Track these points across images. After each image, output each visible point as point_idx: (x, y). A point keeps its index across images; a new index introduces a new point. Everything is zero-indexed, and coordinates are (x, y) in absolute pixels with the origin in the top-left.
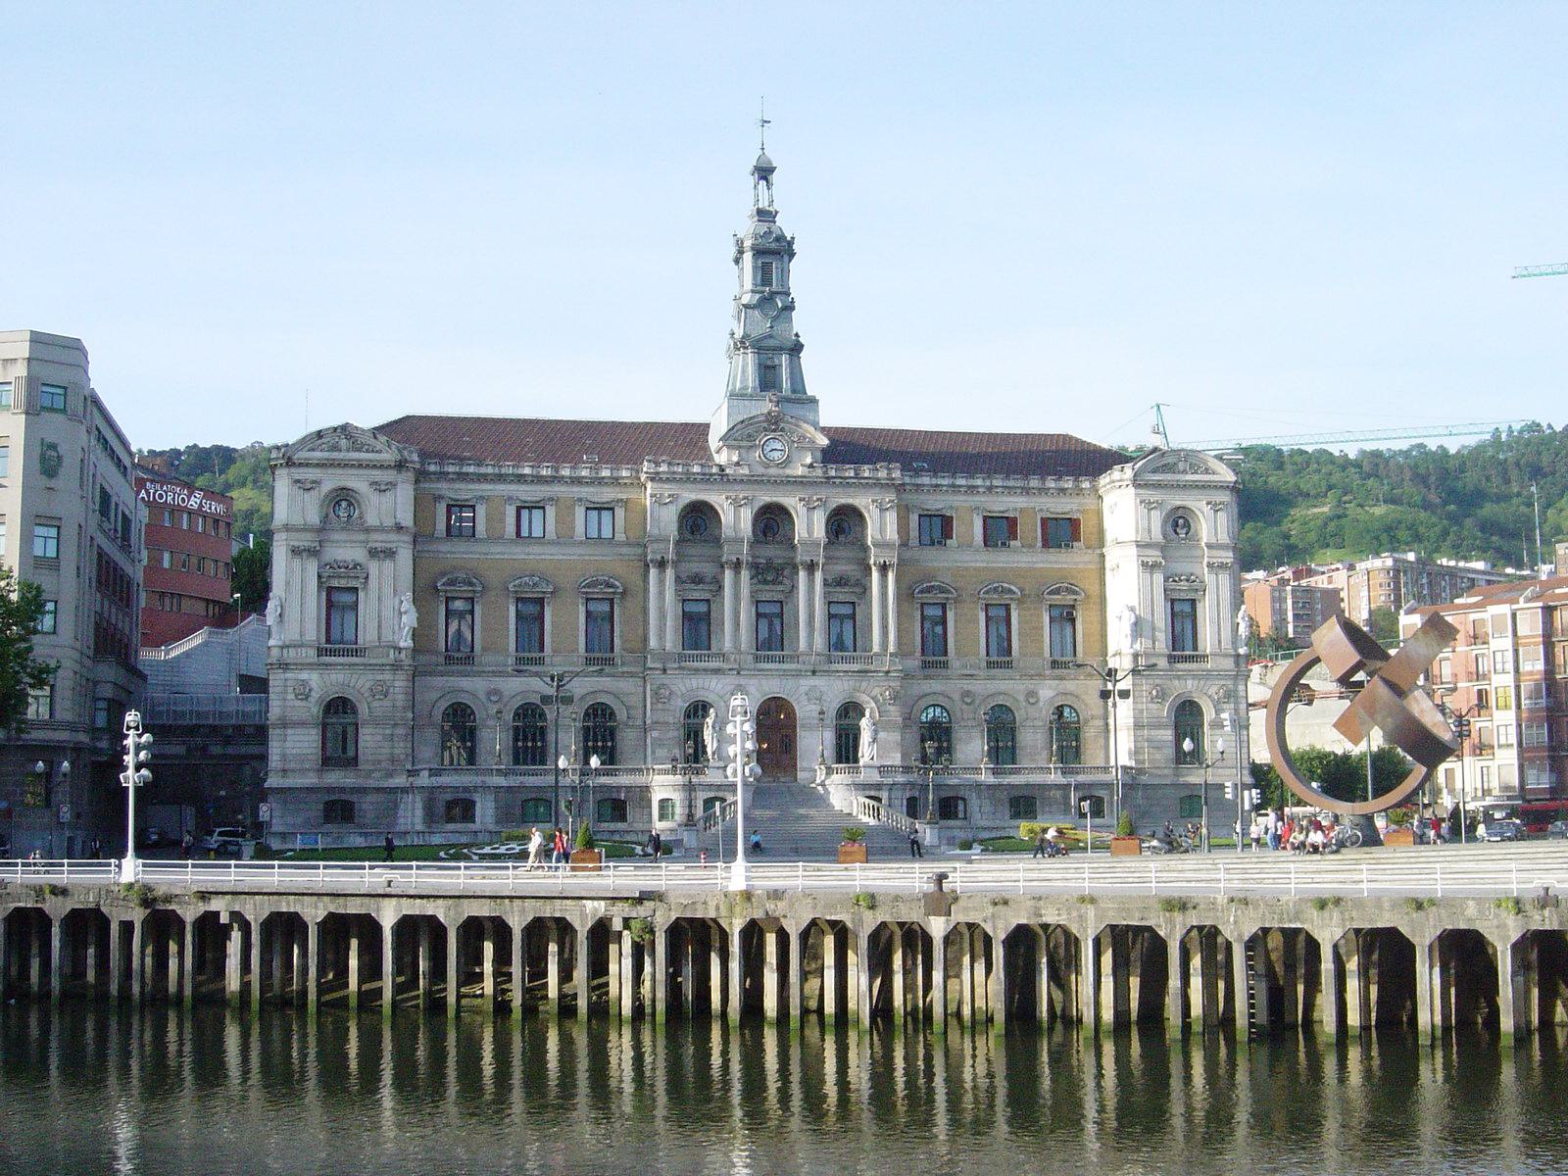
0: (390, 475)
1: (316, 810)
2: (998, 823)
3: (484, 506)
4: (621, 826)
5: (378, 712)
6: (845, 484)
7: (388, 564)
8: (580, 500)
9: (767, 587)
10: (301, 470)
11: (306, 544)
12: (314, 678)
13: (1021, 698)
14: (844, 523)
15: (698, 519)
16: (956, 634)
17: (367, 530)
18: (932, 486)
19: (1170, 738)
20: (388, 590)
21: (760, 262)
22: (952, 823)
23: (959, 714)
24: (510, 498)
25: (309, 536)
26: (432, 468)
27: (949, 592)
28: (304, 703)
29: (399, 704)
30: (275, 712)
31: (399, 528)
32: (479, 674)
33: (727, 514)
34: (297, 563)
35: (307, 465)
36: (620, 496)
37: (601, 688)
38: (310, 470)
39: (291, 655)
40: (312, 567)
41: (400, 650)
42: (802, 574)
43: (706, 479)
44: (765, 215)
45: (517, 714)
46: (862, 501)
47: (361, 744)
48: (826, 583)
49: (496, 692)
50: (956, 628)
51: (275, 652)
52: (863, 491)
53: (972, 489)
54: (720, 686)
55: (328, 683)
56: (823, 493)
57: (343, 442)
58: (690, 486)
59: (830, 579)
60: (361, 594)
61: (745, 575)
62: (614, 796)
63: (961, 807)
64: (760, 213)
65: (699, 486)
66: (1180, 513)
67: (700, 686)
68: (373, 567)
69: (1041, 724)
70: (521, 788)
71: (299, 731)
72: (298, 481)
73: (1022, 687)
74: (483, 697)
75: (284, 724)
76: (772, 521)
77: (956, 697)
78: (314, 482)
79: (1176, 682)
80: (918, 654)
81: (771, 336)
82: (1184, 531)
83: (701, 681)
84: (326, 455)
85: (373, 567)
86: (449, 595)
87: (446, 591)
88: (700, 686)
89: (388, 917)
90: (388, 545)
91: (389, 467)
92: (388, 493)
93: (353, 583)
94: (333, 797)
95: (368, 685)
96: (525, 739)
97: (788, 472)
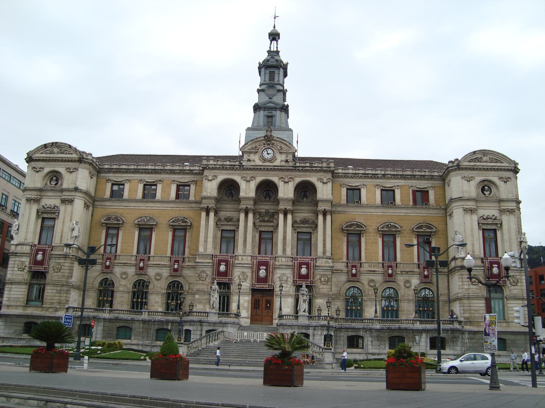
0: (76, 165)
1: (20, 327)
3: (129, 184)
5: (55, 278)
6: (304, 170)
7: (69, 207)
8: (174, 181)
11: (33, 196)
14: (305, 191)
16: (366, 249)
17: (62, 191)
18: (353, 174)
19: (484, 305)
20: (68, 219)
21: (268, 71)
22: (355, 350)
23: (367, 292)
24: (141, 180)
25: (35, 193)
26: (106, 167)
27: (362, 227)
28: (22, 273)
29: (66, 275)
30: (9, 276)
31: (76, 189)
34: (28, 206)
35: (39, 160)
36: (193, 179)
39: (19, 248)
40: (35, 207)
42: (281, 216)
43: (232, 168)
44: (273, 54)
45: (135, 285)
46: (313, 179)
47: (46, 294)
48: (294, 222)
49: (125, 273)
50: (366, 246)
52: (314, 174)
53: (375, 176)
56: (293, 174)
57: (56, 150)
59: (298, 220)
60: (56, 221)
61: (251, 216)
62: (165, 327)
63: (360, 341)
64: (269, 52)
65: (229, 172)
66: (486, 183)
68: (62, 208)
69: (412, 298)
70: (117, 319)
71: (17, 286)
72: (34, 168)
75: (12, 283)
76: (267, 189)
78: (41, 168)
80: (345, 260)
81: (271, 102)
82: (488, 193)
84: (48, 155)
85: (62, 208)
86: (108, 226)
87: (106, 224)
90: (70, 197)
91: (75, 161)
92: (73, 173)
93: (53, 216)
94: (31, 320)
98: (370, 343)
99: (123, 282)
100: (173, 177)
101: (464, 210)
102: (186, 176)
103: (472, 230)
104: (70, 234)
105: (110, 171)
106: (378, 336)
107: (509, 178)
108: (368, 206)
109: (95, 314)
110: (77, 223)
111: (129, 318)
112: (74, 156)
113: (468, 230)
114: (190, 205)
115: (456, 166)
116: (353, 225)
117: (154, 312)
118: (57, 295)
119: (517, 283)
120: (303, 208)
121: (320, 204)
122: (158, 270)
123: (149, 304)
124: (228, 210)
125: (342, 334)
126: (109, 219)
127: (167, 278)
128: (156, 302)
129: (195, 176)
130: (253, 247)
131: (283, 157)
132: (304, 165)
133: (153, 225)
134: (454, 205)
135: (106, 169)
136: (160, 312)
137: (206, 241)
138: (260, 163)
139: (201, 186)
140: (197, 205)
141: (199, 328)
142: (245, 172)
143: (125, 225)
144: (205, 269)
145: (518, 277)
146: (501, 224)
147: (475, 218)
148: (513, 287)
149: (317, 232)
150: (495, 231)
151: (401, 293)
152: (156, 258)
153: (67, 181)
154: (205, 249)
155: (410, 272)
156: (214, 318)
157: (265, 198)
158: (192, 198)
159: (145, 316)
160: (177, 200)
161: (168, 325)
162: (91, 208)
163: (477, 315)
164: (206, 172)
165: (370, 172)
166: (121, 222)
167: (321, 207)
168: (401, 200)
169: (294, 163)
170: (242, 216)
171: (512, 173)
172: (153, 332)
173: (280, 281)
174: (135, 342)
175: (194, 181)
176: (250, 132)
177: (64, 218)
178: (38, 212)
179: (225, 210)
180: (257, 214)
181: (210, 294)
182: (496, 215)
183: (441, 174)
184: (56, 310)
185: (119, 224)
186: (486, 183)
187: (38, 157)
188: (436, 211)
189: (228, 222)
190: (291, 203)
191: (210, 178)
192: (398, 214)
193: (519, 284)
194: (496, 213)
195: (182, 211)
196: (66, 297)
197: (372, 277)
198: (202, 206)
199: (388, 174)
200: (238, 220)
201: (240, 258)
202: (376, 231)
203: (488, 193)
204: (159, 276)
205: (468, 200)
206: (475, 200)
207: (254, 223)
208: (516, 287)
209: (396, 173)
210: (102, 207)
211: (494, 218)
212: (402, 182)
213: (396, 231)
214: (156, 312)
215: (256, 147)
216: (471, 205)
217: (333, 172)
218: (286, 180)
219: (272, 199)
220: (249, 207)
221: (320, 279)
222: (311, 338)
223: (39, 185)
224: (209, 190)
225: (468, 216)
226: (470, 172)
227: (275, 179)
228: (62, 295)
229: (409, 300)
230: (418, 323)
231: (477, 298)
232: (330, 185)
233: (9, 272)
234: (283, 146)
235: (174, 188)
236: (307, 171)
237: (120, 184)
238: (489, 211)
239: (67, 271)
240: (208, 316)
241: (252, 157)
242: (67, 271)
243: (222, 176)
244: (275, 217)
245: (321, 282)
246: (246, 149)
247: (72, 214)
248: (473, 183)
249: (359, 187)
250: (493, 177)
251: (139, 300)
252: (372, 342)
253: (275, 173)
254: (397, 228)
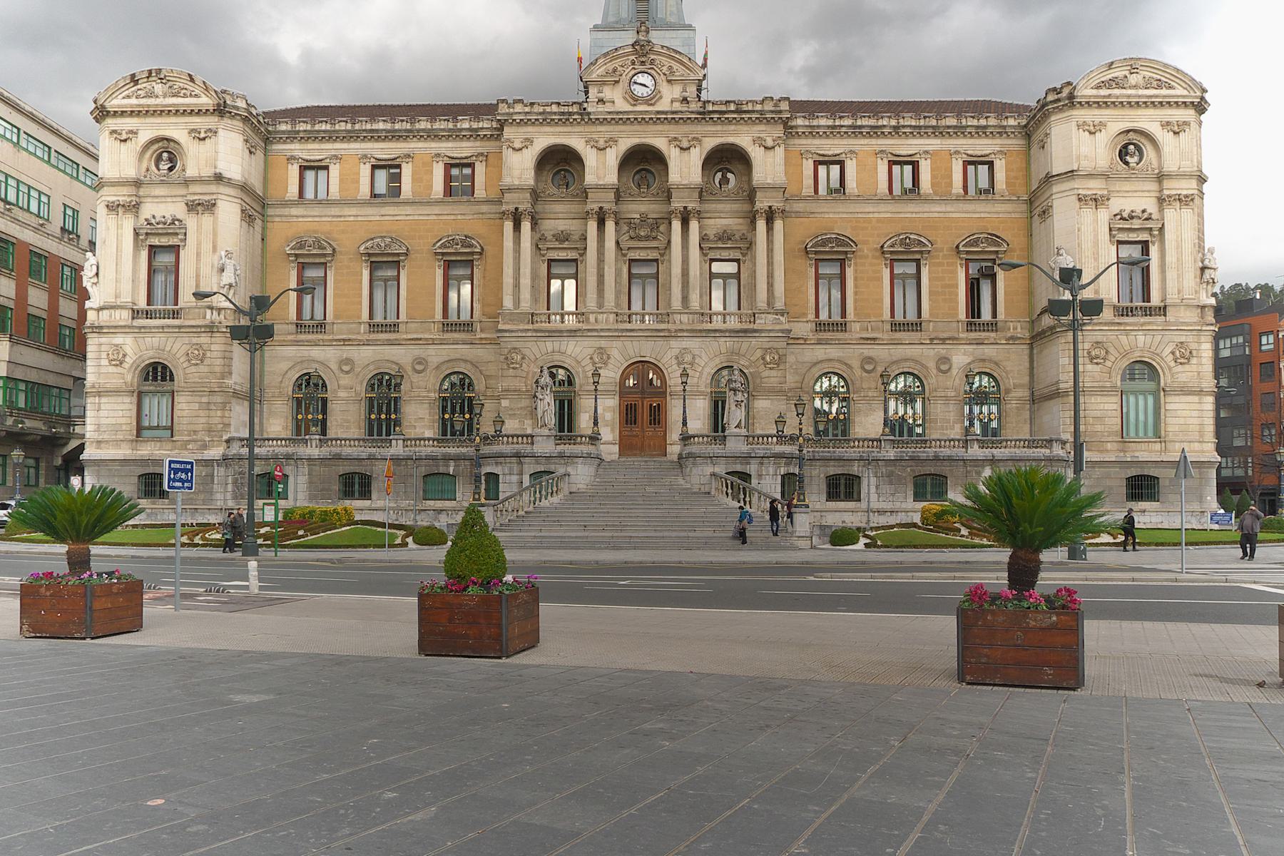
2: (898, 505)
4: (448, 504)
7: (206, 219)
8: (438, 155)
9: (641, 244)
10: (119, 120)
12: (128, 343)
13: (932, 364)
15: (560, 162)
16: (856, 293)
17: (187, 182)
18: (829, 127)
22: (842, 505)
23: (858, 383)
24: (365, 156)
26: (283, 127)
27: (848, 245)
28: (119, 370)
29: (217, 369)
31: (219, 178)
32: (329, 343)
33: (590, 158)
36: (480, 150)
37: (458, 356)
38: (128, 120)
40: (128, 223)
41: (219, 310)
42: (676, 225)
43: (565, 119)
45: (371, 387)
46: (743, 138)
48: (703, 238)
49: (348, 361)
50: (856, 286)
51: (91, 316)
52: (746, 128)
53: (875, 132)
54: (578, 349)
55: (143, 348)
57: (159, 88)
58: (547, 129)
59: (711, 233)
60: (182, 252)
67: (557, 349)
68: (191, 222)
70: (337, 457)
72: (114, 132)
73: (932, 353)
74: (334, 367)
77: (856, 364)
78: (131, 132)
79: (1123, 338)
80: (811, 316)
82: (1136, 159)
83: (556, 345)
85: (191, 222)
86: (301, 260)
87: (296, 255)
88: (557, 349)
90: (207, 198)
95: (185, 348)
96: (379, 413)
97: (658, 108)
98: (873, 489)
99: (345, 380)
100: (435, 146)
101: (1080, 200)
102: (465, 144)
103: (1096, 243)
104: (215, 280)
105: (292, 137)
106: (890, 475)
107: (1185, 123)
108: (859, 199)
109: (290, 450)
110: (228, 253)
111: (364, 455)
112: (206, 101)
113: (1087, 245)
114: (476, 208)
115: (1063, 99)
116: (829, 240)
117: (416, 440)
118: (202, 413)
119: (1188, 359)
120: (720, 206)
121: (759, 194)
122: (417, 351)
123: (405, 423)
124: (561, 216)
125: (815, 473)
126: (301, 245)
127: (437, 368)
128: (420, 418)
129: (483, 144)
130: (617, 297)
131: (676, 91)
132: (723, 108)
133: (398, 255)
134: (1055, 189)
135: (283, 132)
136: (429, 439)
137: (517, 285)
138: (628, 108)
139: (499, 166)
140: (494, 208)
141: (516, 468)
142: (593, 128)
143: (338, 256)
144: (518, 345)
145: (1193, 346)
146: (1161, 229)
147: (1104, 216)
148: (1180, 368)
149: (753, 259)
150: (1145, 246)
151: (932, 381)
152: (413, 325)
153: (196, 160)
154: (517, 302)
155: (949, 339)
156: (545, 446)
157: (639, 186)
158: (480, 192)
159: (397, 449)
160: (450, 199)
161: (448, 466)
162: (258, 222)
163: (1099, 428)
164: (508, 132)
165: (865, 122)
166: (329, 251)
167: (762, 203)
168: (933, 185)
169: (700, 104)
170: (592, 226)
171: (1192, 112)
172: (417, 482)
173: (679, 364)
174: (380, 504)
175: (482, 154)
176: (600, 35)
177: (199, 244)
178: (136, 234)
179: (552, 216)
180: (621, 222)
181: (535, 396)
182: (1149, 211)
183: (1024, 122)
184: (205, 447)
185: (324, 255)
186: (1131, 135)
187: (119, 106)
188: (1008, 207)
189: (562, 241)
190: (696, 195)
191: (517, 145)
192: (926, 215)
193: (1194, 361)
194: (1152, 207)
195: (460, 219)
196: (223, 417)
197: (868, 350)
198: (504, 208)
199: (904, 127)
200: (584, 238)
201: (592, 318)
202: (878, 254)
203: (1136, 159)
204: (419, 363)
205: (1090, 176)
206: (1105, 176)
207: (617, 243)
208: (1187, 366)
209: (922, 122)
210: (284, 219)
211: (1146, 215)
212: (933, 144)
213: (921, 252)
214: (420, 440)
215: (615, 70)
216: (1095, 187)
217: (785, 123)
218: (685, 145)
219: (654, 189)
220: (606, 206)
221: (763, 359)
222: (754, 481)
223: (131, 172)
224: (516, 173)
225: (1088, 213)
226: (1097, 112)
227: (660, 143)
228: (212, 413)
229: (947, 398)
230: (976, 446)
231: (1102, 391)
232: (780, 151)
233: (89, 370)
234: (676, 66)
235: (438, 171)
236: (729, 121)
237: (319, 167)
238: (1137, 199)
239: (219, 362)
240: (532, 443)
241: (608, 93)
242: (219, 362)
243: (544, 139)
244: (662, 228)
245: (766, 364)
246: (594, 77)
247: (215, 234)
248: (1103, 138)
249: (842, 157)
250: (1148, 121)
251: (383, 416)
252: (877, 487)
253: (660, 127)
254: (925, 245)
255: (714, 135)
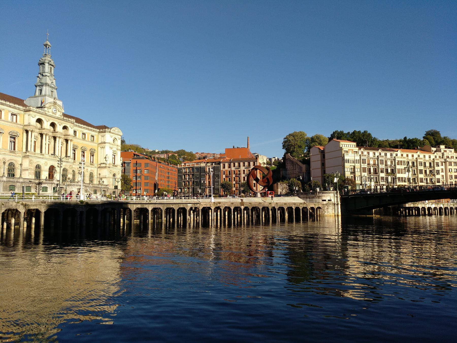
6: (66, 121)
89: (150, 208)
102: (16, 110)
127: (8, 161)
231: (111, 178)
241: (50, 110)
243: (38, 116)
248: (112, 139)
255: (64, 123)
